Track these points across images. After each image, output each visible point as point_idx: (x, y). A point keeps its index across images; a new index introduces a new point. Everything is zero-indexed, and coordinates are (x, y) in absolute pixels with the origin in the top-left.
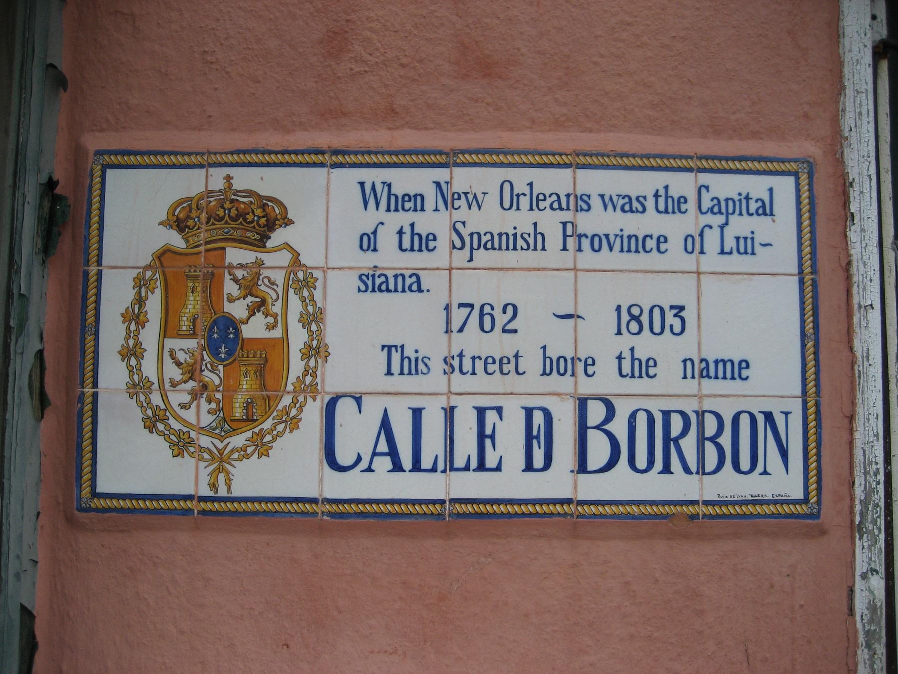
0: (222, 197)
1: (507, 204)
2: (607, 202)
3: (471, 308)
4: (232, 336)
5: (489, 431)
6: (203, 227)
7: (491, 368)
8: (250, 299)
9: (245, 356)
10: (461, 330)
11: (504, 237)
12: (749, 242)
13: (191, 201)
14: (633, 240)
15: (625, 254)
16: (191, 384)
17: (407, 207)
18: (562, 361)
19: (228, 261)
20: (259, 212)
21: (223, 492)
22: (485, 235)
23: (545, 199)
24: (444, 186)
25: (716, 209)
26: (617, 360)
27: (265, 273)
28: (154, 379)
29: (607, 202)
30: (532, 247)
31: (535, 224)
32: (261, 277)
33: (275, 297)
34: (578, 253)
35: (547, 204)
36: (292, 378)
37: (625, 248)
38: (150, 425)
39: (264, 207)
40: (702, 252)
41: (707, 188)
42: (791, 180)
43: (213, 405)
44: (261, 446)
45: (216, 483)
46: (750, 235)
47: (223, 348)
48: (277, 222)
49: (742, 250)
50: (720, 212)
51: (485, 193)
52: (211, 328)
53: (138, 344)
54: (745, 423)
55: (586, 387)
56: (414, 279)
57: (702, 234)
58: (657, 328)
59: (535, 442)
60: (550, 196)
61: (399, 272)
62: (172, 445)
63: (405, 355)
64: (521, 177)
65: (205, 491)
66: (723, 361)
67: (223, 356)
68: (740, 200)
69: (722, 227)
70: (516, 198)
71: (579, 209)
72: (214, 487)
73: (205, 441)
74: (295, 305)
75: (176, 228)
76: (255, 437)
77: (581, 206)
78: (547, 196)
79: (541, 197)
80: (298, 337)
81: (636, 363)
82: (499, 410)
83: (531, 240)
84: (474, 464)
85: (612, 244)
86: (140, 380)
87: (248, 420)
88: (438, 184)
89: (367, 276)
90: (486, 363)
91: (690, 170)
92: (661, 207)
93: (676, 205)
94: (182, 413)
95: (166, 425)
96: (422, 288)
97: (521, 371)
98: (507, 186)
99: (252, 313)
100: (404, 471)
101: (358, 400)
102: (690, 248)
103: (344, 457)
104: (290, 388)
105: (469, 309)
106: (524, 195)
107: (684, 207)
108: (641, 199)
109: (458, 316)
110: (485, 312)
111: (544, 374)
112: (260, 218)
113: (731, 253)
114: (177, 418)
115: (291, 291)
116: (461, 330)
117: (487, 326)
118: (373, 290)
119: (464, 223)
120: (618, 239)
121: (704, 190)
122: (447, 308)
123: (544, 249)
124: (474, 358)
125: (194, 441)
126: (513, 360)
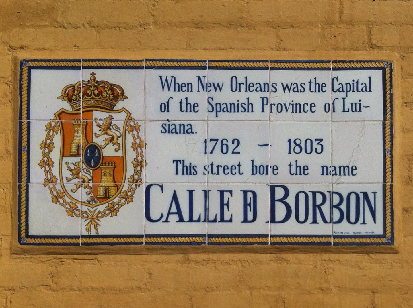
0: (90, 84)
1: (234, 89)
2: (286, 88)
4: (97, 155)
5: (225, 202)
6: (81, 100)
7: (227, 171)
8: (107, 137)
10: (211, 152)
11: (233, 106)
12: (358, 105)
13: (74, 86)
14: (298, 106)
15: (294, 113)
16: (77, 180)
18: (262, 168)
19: (94, 117)
23: (253, 86)
25: (341, 90)
26: (289, 166)
27: (113, 122)
28: (58, 177)
29: (286, 88)
31: (248, 99)
32: (112, 125)
34: (271, 113)
35: (254, 88)
36: (128, 176)
37: (294, 111)
38: (56, 199)
39: (112, 89)
40: (334, 111)
41: (337, 78)
42: (380, 72)
43: (88, 190)
44: (113, 210)
45: (90, 228)
46: (359, 102)
47: (92, 161)
49: (354, 110)
50: (343, 91)
52: (87, 150)
54: (353, 197)
55: (275, 180)
57: (333, 103)
58: (309, 150)
59: (248, 207)
60: (256, 85)
63: (185, 164)
64: (241, 75)
65: (86, 233)
66: (343, 166)
67: (93, 165)
68: (354, 84)
69: (344, 99)
72: (88, 230)
73: (85, 208)
76: (110, 205)
78: (255, 84)
79: (251, 85)
80: (131, 155)
82: (231, 192)
83: (246, 107)
84: (218, 219)
85: (287, 108)
86: (52, 178)
89: (166, 125)
90: (224, 169)
92: (313, 89)
93: (320, 88)
96: (193, 131)
97: (241, 173)
98: (234, 79)
99: (107, 143)
100: (185, 222)
101: (162, 187)
102: (327, 110)
103: (154, 215)
104: (127, 181)
105: (215, 142)
108: (303, 85)
111: (253, 174)
113: (348, 111)
114: (71, 197)
115: (127, 132)
116: (211, 152)
117: (225, 150)
118: (169, 132)
119: (212, 99)
120: (291, 105)
121: (335, 80)
122: (206, 141)
123: (252, 111)
124: (218, 167)
126: (237, 167)
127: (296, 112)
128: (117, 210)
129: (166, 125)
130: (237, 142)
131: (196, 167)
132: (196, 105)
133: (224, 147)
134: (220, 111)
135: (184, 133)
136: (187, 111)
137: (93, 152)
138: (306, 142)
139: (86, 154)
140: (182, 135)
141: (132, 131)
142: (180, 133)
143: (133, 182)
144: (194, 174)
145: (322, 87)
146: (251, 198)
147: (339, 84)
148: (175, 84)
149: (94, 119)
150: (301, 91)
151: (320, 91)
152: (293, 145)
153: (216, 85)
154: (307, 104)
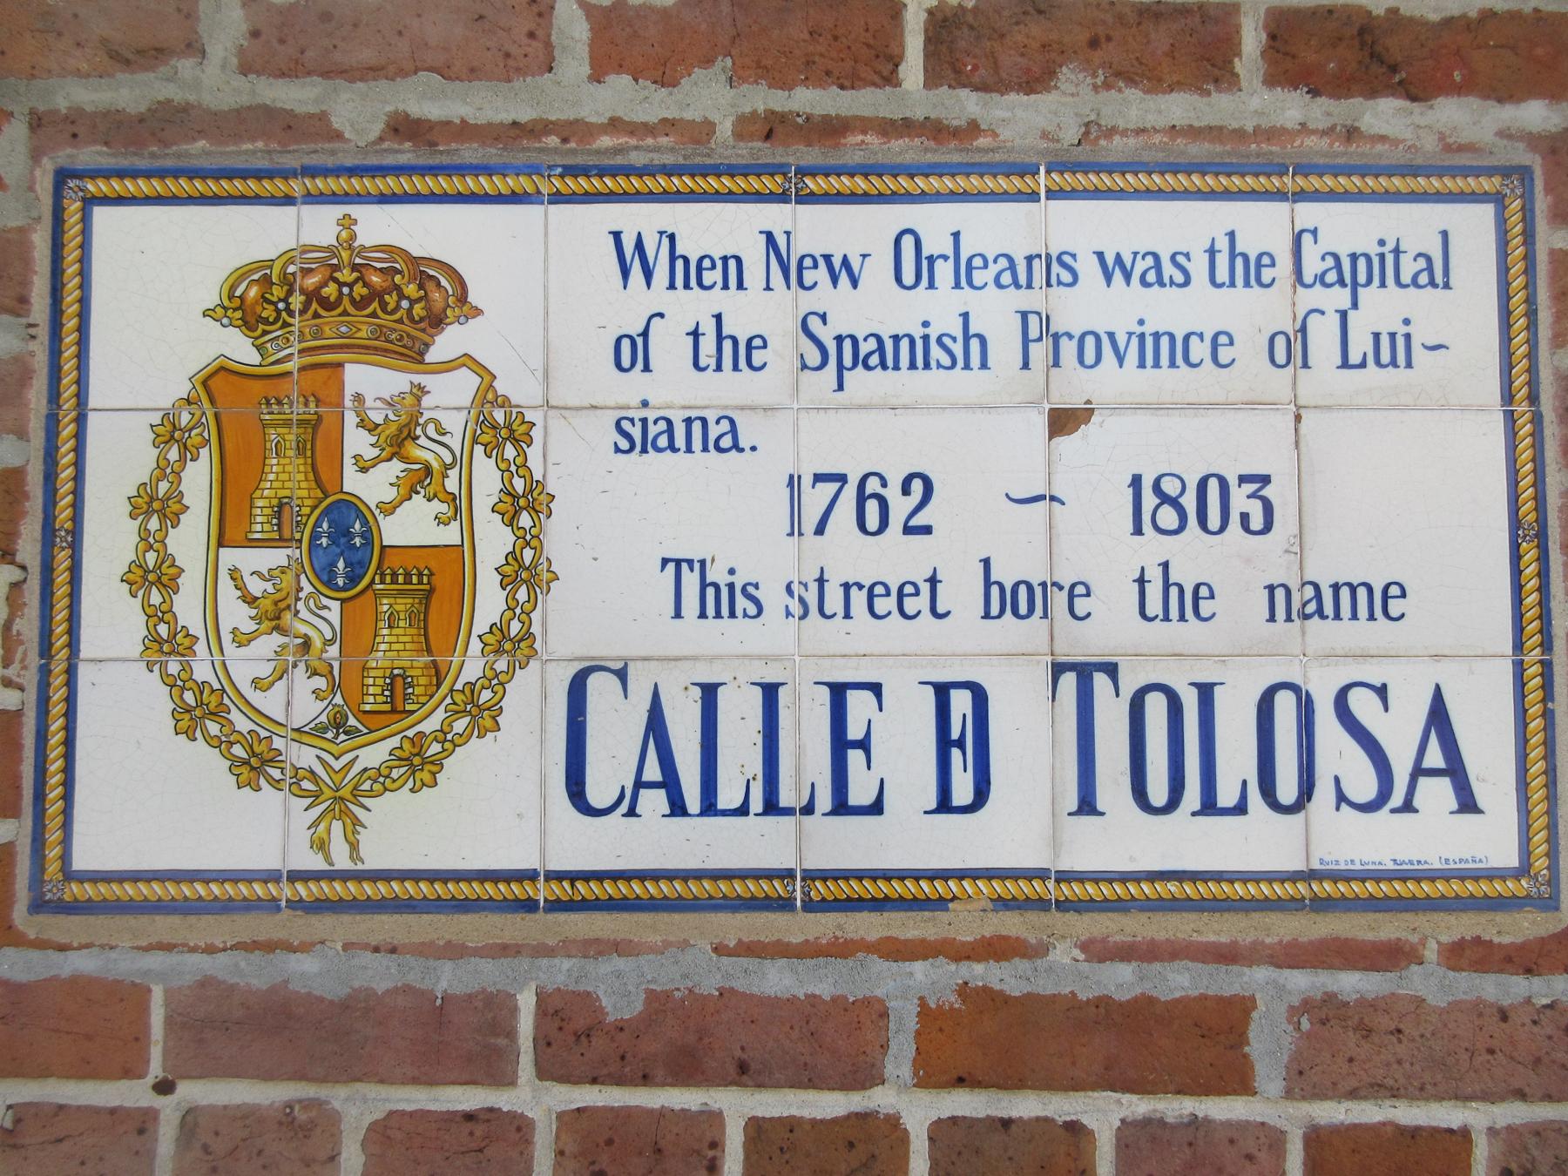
0: (335, 261)
1: (909, 278)
2: (1113, 268)
3: (839, 484)
4: (358, 541)
7: (882, 605)
8: (396, 467)
9: (388, 579)
10: (820, 530)
11: (905, 344)
14: (1165, 341)
16: (277, 639)
17: (706, 282)
18: (1023, 590)
19: (349, 391)
20: (411, 290)
21: (342, 861)
22: (865, 340)
23: (986, 266)
24: (781, 241)
25: (1331, 277)
26: (1136, 584)
27: (427, 415)
28: (197, 629)
29: (1113, 268)
30: (960, 363)
31: (965, 316)
33: (449, 460)
34: (1054, 371)
36: (481, 626)
40: (1305, 365)
41: (1314, 232)
42: (1487, 211)
43: (320, 683)
46: (1402, 330)
47: (341, 564)
48: (449, 312)
49: (1385, 357)
50: (1342, 282)
51: (864, 256)
52: (317, 524)
53: (166, 558)
56: (725, 425)
57: (1303, 329)
58: (1214, 521)
60: (995, 261)
61: (694, 414)
62: (236, 764)
66: (1349, 584)
67: (340, 582)
68: (1382, 257)
69: (1344, 315)
70: (926, 266)
71: (1054, 280)
72: (321, 846)
73: (305, 757)
74: (487, 479)
75: (240, 322)
76: (407, 745)
79: (978, 262)
80: (493, 541)
81: (1174, 591)
83: (958, 349)
85: (1122, 349)
87: (394, 711)
88: (770, 237)
89: (632, 421)
90: (871, 597)
91: (1279, 195)
92: (1222, 274)
94: (256, 698)
95: (223, 726)
97: (940, 610)
98: (908, 242)
102: (1281, 357)
104: (475, 645)
105: (835, 486)
106: (945, 258)
107: (1267, 274)
108: (1180, 259)
109: (816, 499)
110: (868, 491)
111: (987, 616)
112: (413, 302)
113: (1363, 365)
116: (820, 530)
117: (872, 522)
119: (823, 318)
120: (1135, 341)
121: (1307, 239)
122: (793, 482)
123: (984, 365)
124: (847, 587)
125: (281, 755)
126: (925, 588)
127: (1157, 365)
128: (438, 763)
129: (632, 421)
130: (922, 485)
131: (756, 586)
132: (755, 343)
133: (872, 507)
134: (855, 365)
135: (705, 449)
136: (719, 368)
137: (341, 533)
138: (1202, 485)
139: (315, 536)
141: (499, 446)
143: (499, 651)
144: (745, 615)
146: (964, 715)
147: (1323, 258)
148: (673, 258)
149: (348, 403)
150: (1172, 283)
151: (1253, 282)
152: (1149, 500)
153: (837, 262)
154: (1201, 336)
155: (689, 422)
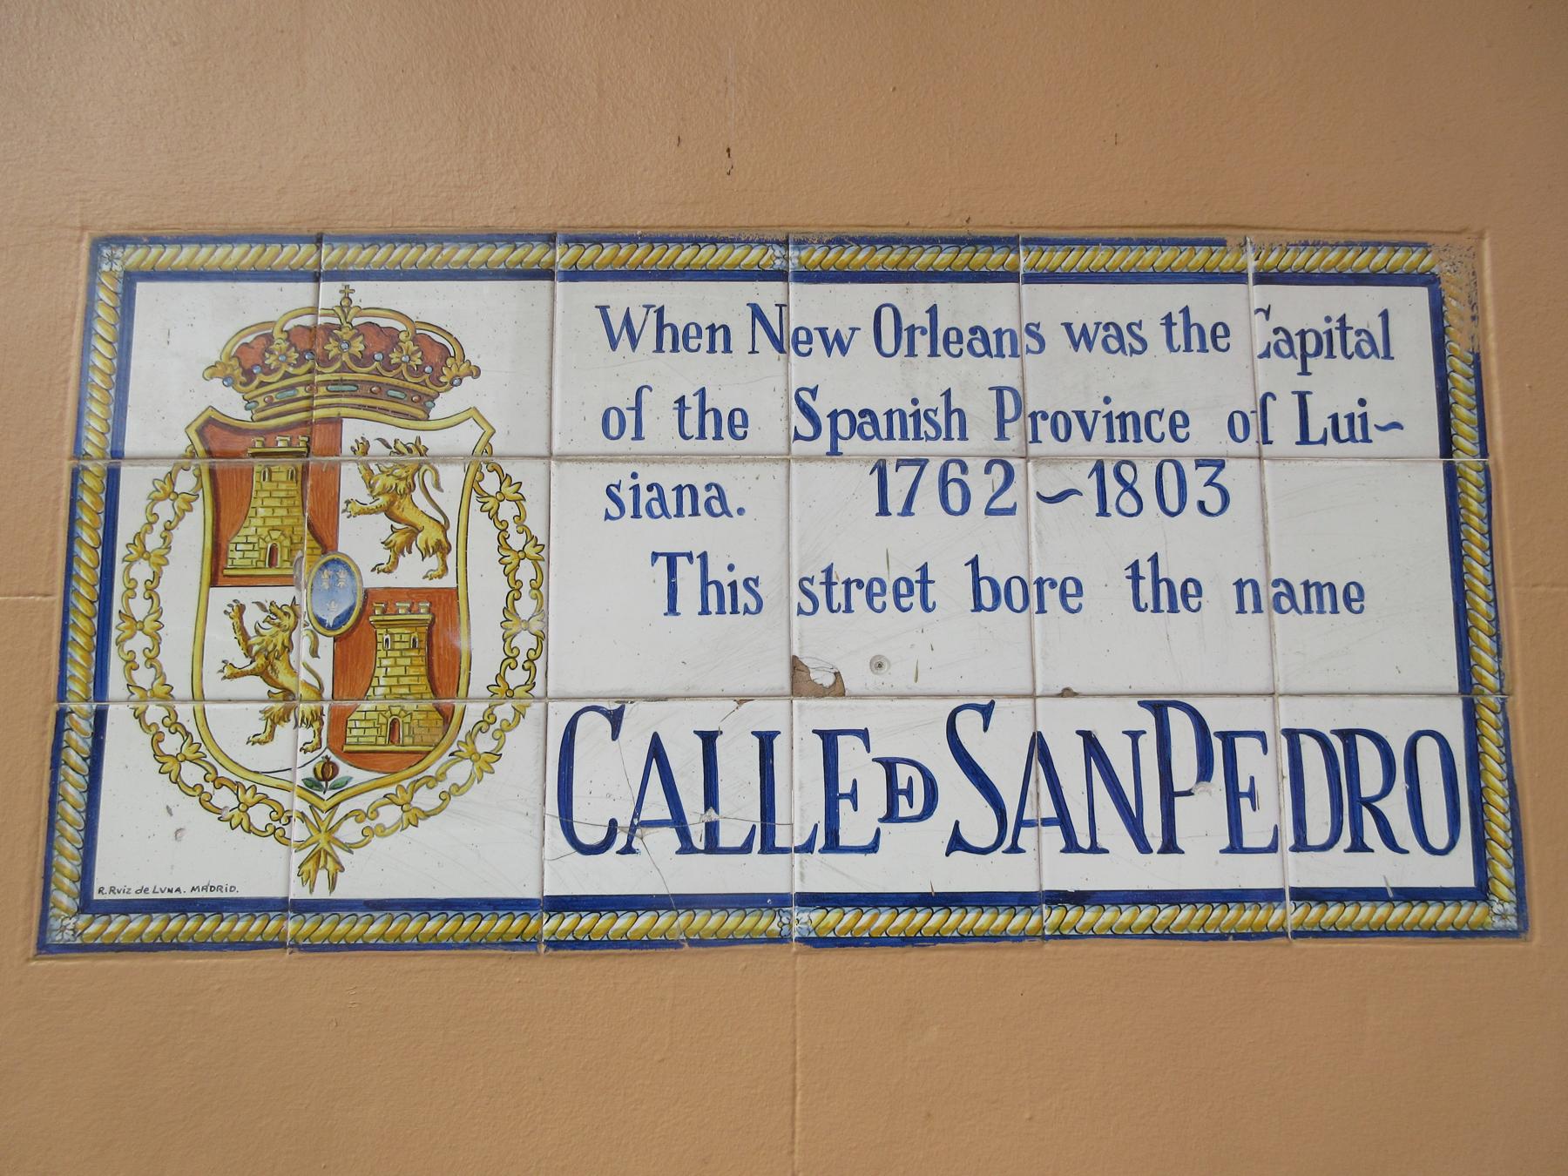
2: (1080, 338)
77: (1027, 346)
135: (695, 513)
140: (687, 520)
142: (679, 514)
145: (1214, 337)
148: (660, 327)
155: (679, 489)
